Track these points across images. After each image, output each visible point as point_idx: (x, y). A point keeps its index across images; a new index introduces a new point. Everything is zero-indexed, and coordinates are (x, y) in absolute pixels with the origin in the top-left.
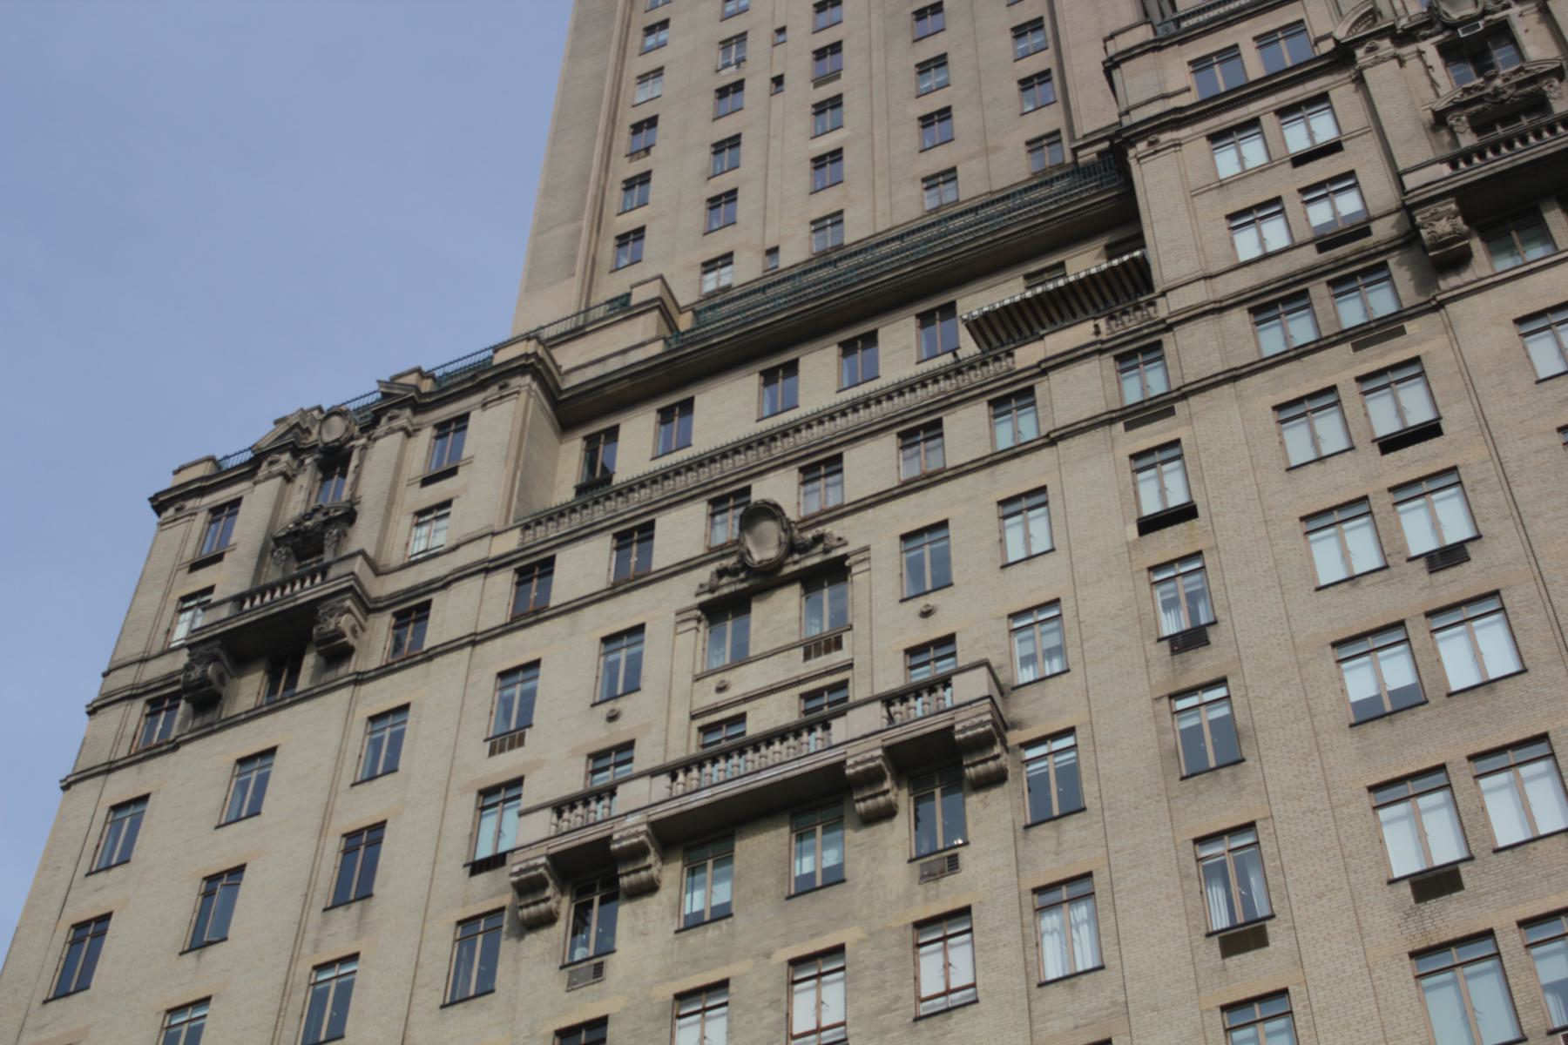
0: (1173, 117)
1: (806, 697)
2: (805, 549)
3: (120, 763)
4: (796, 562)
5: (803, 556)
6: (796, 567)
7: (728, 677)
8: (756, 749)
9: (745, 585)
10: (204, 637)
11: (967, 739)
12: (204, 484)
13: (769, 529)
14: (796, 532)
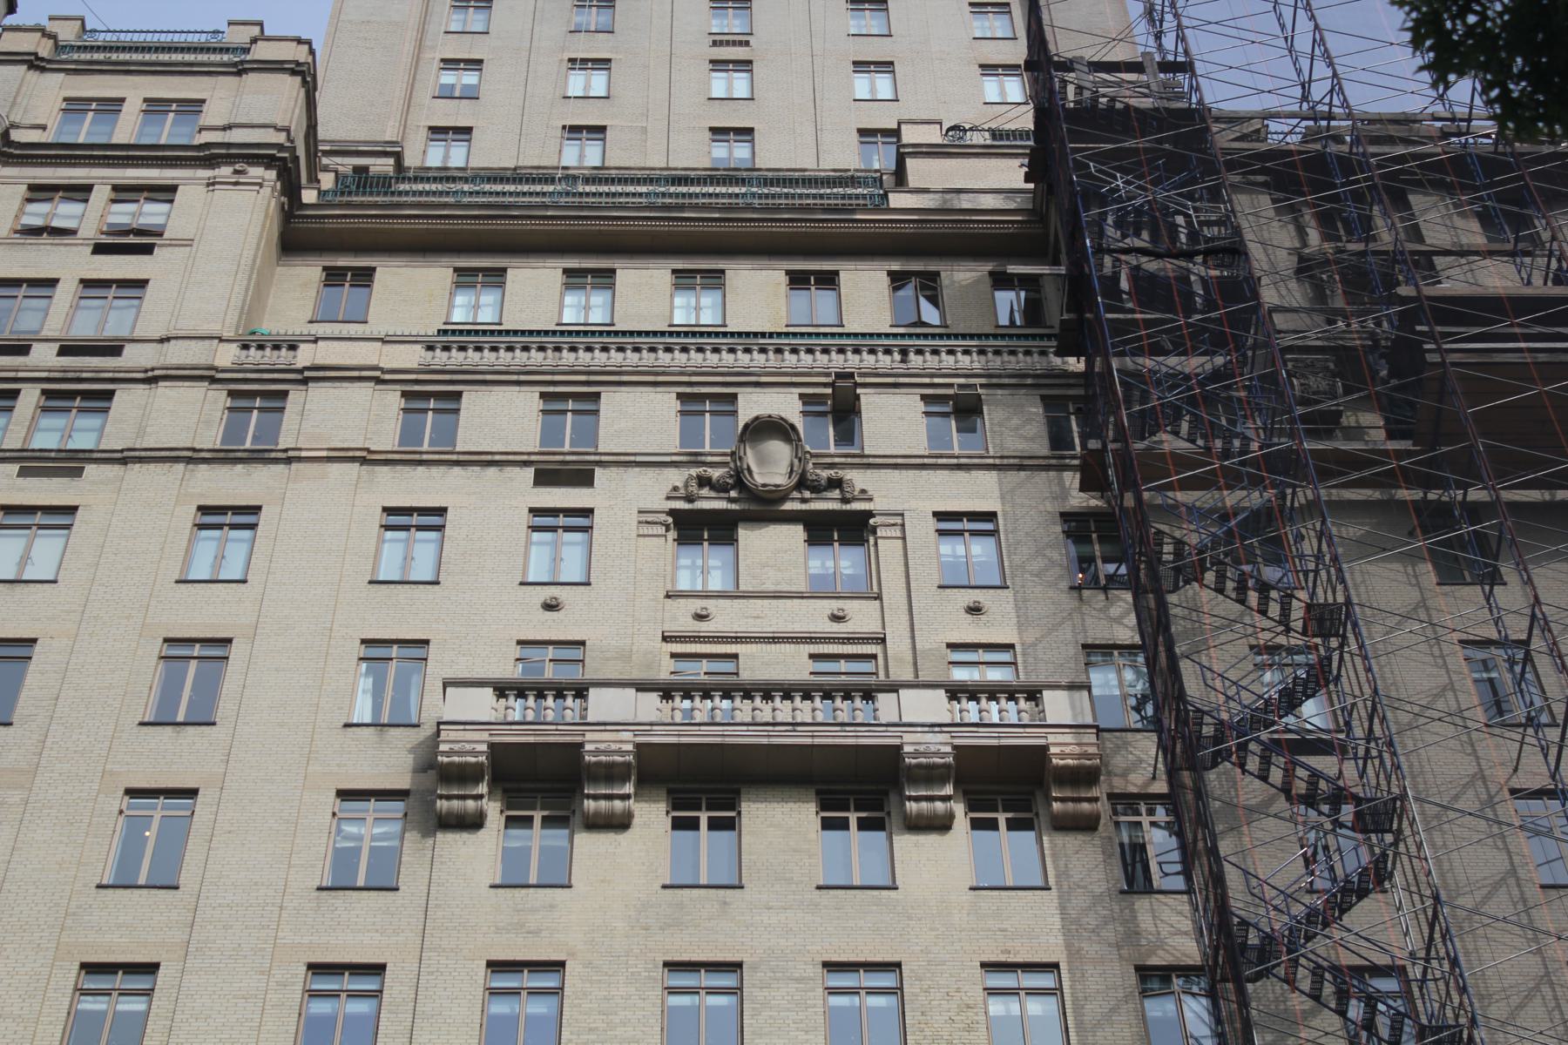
2: (817, 489)
4: (804, 501)
5: (814, 496)
6: (804, 507)
7: (850, 607)
8: (541, 695)
9: (734, 506)
11: (919, 766)
13: (779, 450)
14: (811, 465)
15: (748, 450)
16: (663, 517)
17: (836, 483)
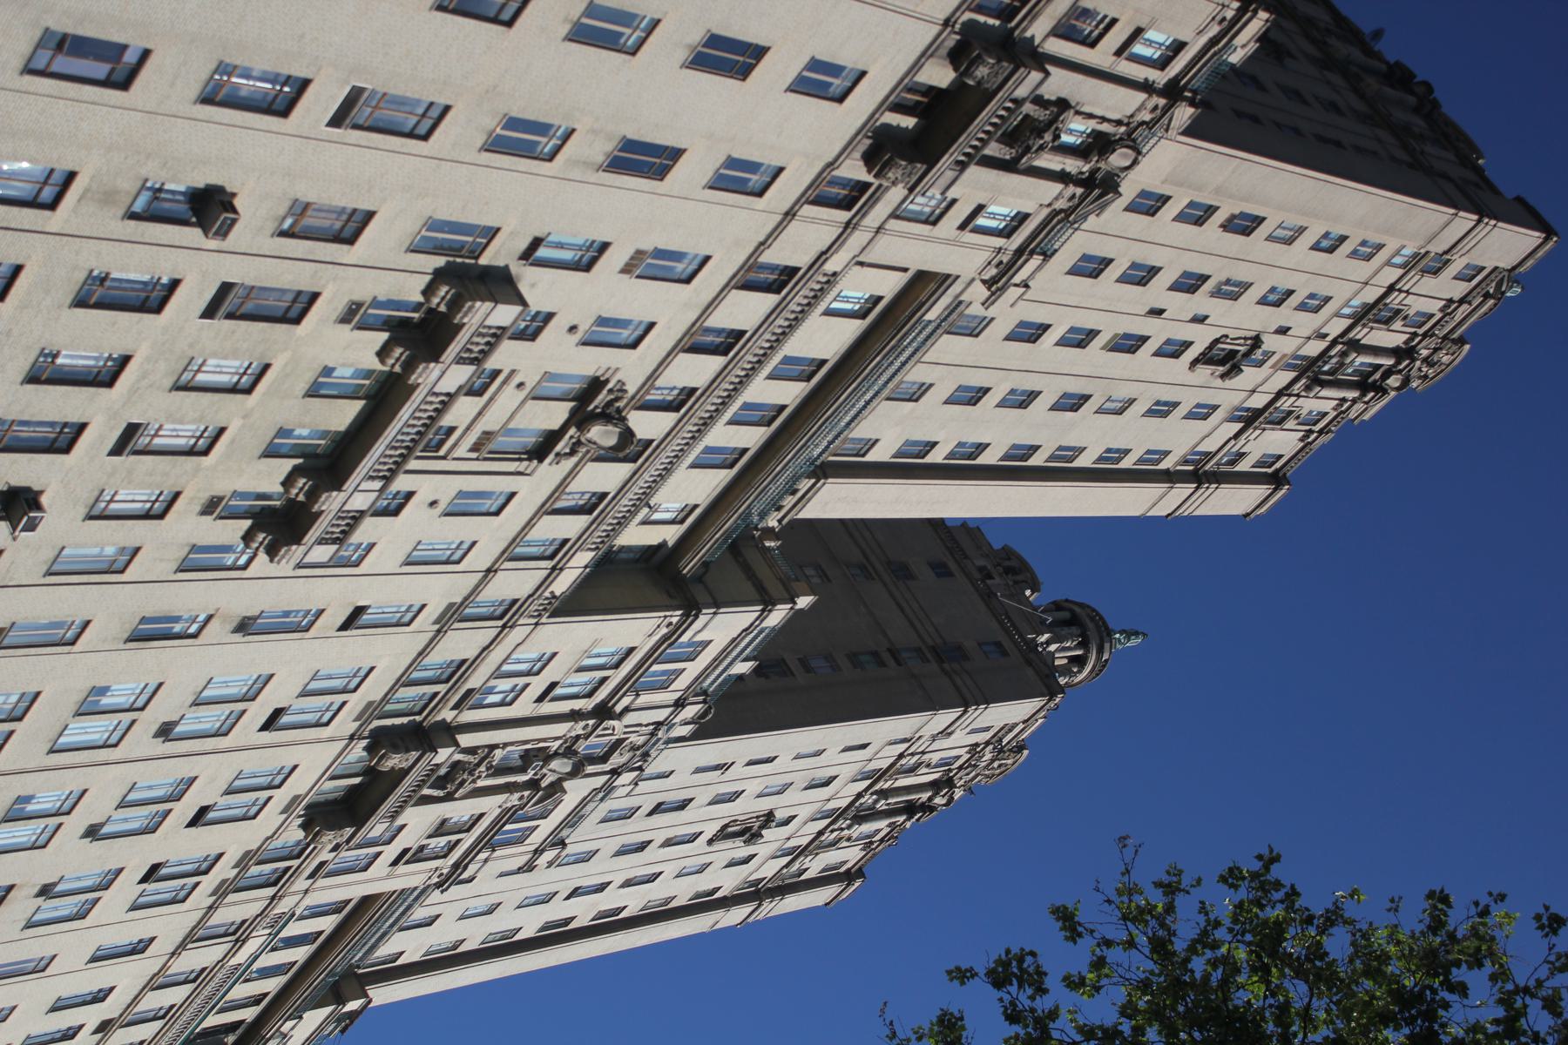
0: (672, 639)
1: (451, 430)
3: (923, 60)
4: (571, 437)
6: (567, 437)
9: (591, 407)
10: (1010, 83)
12: (1216, 48)
15: (618, 430)
16: (606, 376)
17: (573, 452)
